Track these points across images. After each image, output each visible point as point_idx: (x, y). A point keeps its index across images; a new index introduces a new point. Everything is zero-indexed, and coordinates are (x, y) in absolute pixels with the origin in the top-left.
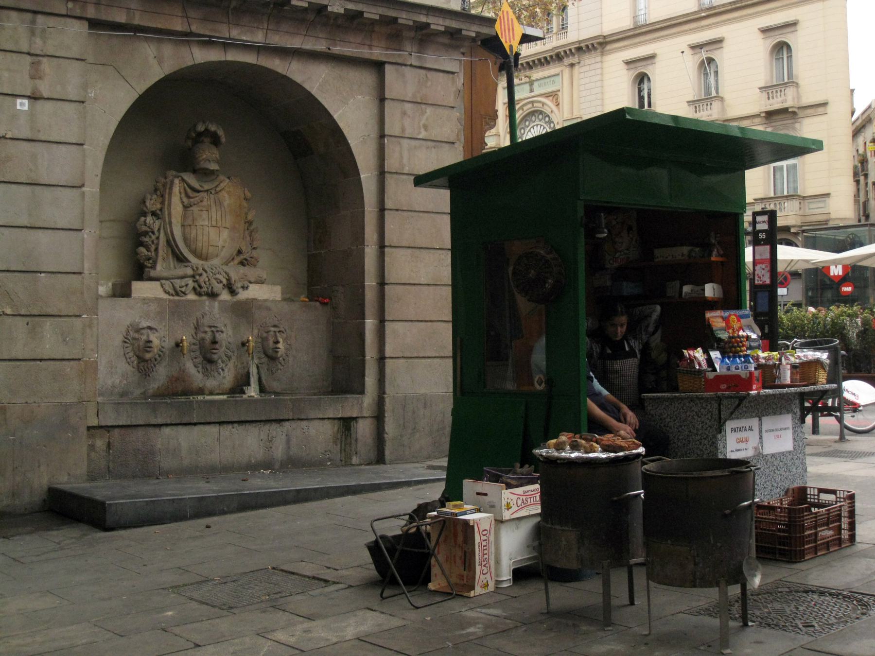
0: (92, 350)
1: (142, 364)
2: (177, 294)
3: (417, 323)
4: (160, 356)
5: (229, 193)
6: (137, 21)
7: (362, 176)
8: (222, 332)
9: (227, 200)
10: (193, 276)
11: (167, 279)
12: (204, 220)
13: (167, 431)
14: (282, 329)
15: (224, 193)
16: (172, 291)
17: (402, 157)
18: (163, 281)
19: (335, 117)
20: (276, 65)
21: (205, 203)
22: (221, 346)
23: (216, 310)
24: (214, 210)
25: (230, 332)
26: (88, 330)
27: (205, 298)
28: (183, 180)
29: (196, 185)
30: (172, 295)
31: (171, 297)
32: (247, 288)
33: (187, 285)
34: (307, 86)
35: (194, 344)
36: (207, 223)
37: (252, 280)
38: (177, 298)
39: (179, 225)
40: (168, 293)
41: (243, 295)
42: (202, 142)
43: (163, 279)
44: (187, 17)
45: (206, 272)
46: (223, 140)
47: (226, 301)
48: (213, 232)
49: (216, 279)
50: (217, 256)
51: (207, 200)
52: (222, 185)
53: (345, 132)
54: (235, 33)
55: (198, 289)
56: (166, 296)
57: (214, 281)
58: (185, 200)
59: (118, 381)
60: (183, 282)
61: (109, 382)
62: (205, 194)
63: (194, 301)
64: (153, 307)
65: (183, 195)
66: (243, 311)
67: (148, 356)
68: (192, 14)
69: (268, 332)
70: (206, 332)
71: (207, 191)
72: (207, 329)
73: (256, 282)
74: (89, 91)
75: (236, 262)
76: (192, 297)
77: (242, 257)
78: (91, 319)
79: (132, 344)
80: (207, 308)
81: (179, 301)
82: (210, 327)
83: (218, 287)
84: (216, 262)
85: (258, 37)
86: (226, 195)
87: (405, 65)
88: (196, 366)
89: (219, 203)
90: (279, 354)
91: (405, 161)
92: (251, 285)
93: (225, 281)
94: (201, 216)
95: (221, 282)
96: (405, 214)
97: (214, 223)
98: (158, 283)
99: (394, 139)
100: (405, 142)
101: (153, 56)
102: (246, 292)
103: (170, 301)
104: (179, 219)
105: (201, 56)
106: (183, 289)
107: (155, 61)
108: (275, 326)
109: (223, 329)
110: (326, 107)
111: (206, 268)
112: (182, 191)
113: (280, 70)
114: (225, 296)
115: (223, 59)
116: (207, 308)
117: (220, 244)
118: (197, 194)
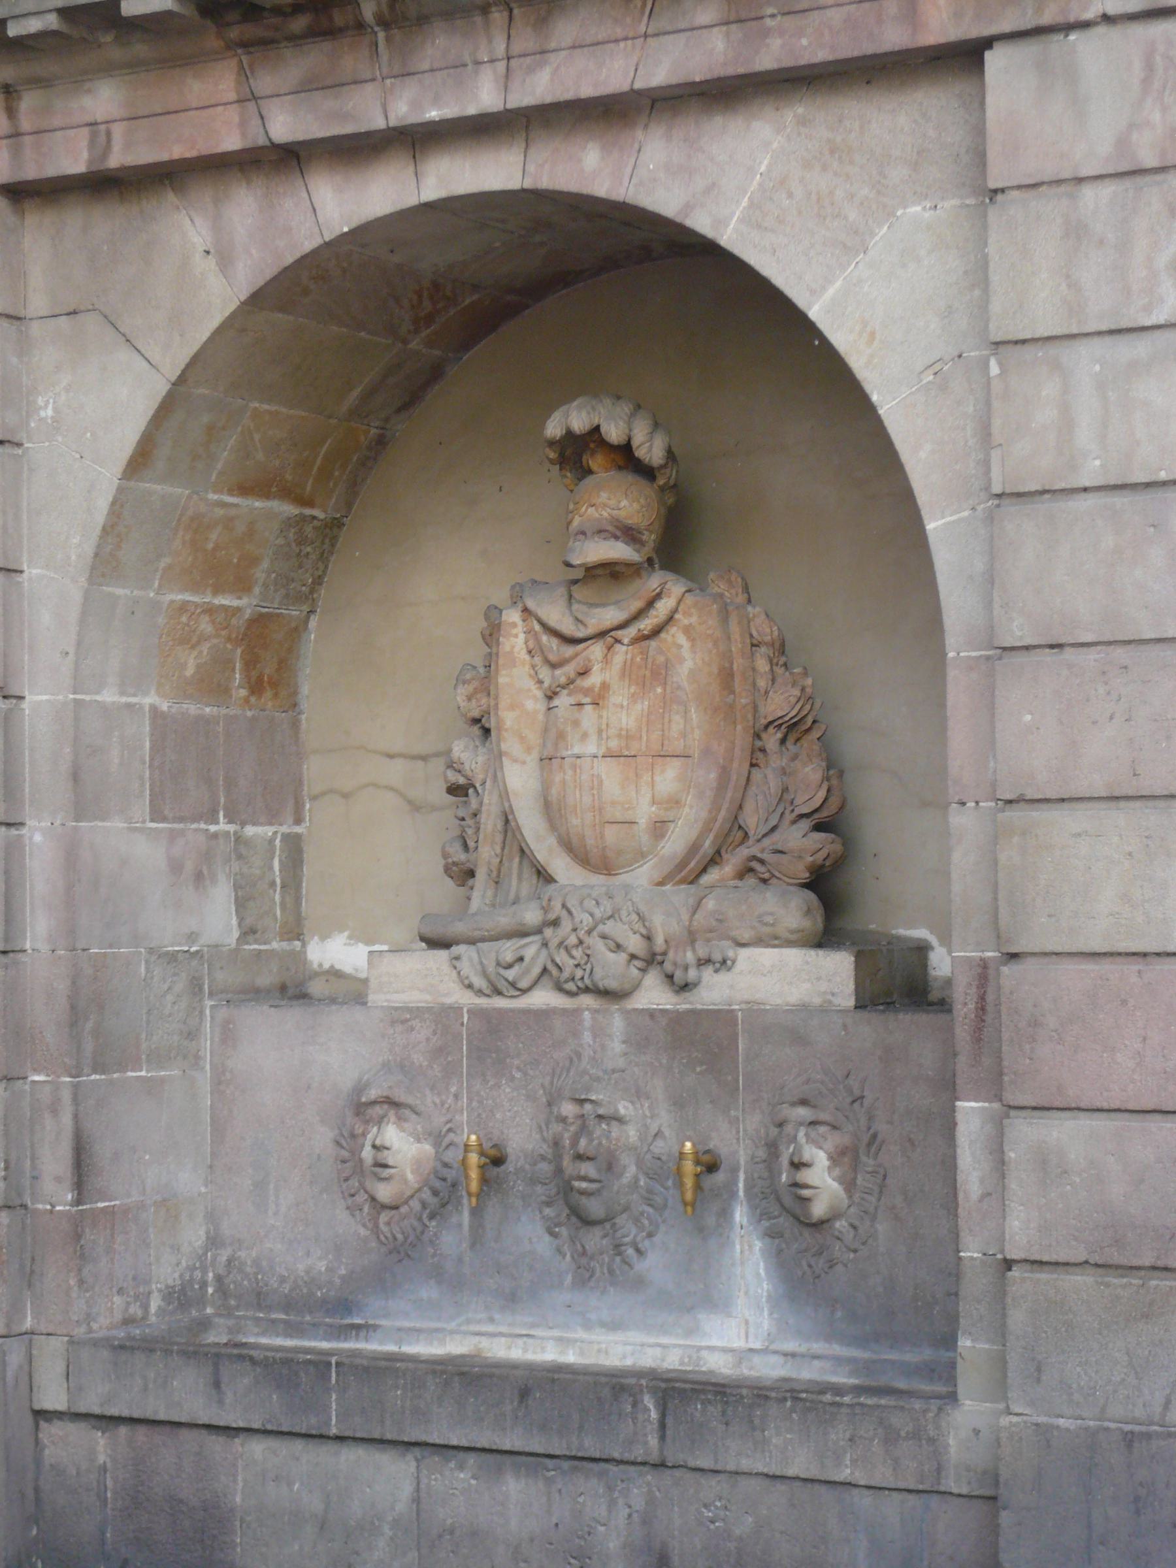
0: (58, 1179)
1: (384, 1217)
2: (499, 993)
3: (1155, 1124)
4: (435, 1193)
5: (687, 630)
6: (116, 160)
7: (930, 526)
8: (620, 1120)
9: (688, 655)
10: (539, 931)
11: (472, 942)
12: (585, 736)
13: (257, 1448)
14: (823, 1116)
15: (675, 636)
16: (479, 982)
17: (1067, 424)
18: (456, 950)
19: (814, 314)
20: (589, 168)
21: (594, 679)
22: (611, 1167)
23: (617, 1046)
24: (619, 696)
25: (664, 1119)
26: (49, 1121)
27: (587, 1000)
28: (525, 610)
29: (568, 627)
30: (480, 993)
31: (482, 1002)
32: (724, 962)
33: (521, 959)
34: (701, 223)
35: (543, 1158)
36: (591, 748)
37: (746, 935)
38: (500, 1003)
39: (532, 759)
40: (470, 986)
41: (715, 990)
42: (590, 472)
43: (457, 944)
44: (255, 98)
45: (570, 912)
46: (651, 450)
47: (652, 1014)
48: (610, 775)
49: (604, 937)
50: (643, 855)
51: (605, 667)
52: (663, 607)
53: (858, 363)
54: (409, 105)
55: (555, 972)
56: (467, 999)
57: (599, 946)
58: (545, 673)
59: (322, 1266)
60: (508, 950)
61: (301, 1267)
62: (596, 650)
63: (542, 1015)
64: (423, 1032)
65: (538, 660)
66: (702, 1045)
67: (384, 1192)
68: (264, 82)
69: (780, 1125)
70: (563, 1120)
71: (602, 634)
72: (568, 1109)
73: (759, 941)
74: (40, 401)
75: (728, 868)
76: (543, 998)
77: (744, 852)
78: (56, 1086)
79: (352, 1153)
80: (587, 1037)
81: (501, 1012)
82: (581, 1102)
83: (611, 967)
84: (642, 876)
85: (485, 96)
86: (682, 640)
87: (1085, 25)
88: (552, 1234)
89: (660, 674)
90: (818, 1210)
91: (1085, 436)
92: (745, 957)
93: (634, 943)
94: (576, 723)
95: (619, 947)
96: (1091, 657)
97: (614, 744)
98: (443, 954)
99: (1028, 352)
100: (1086, 360)
101: (201, 249)
102: (723, 978)
103: (474, 1012)
104: (533, 737)
105: (339, 205)
106: (510, 974)
107: (211, 262)
108: (804, 1102)
109: (623, 1108)
110: (779, 279)
111: (572, 903)
112: (531, 644)
113: (602, 188)
114: (653, 995)
115: (411, 200)
116: (587, 1037)
117: (645, 813)
118: (569, 650)
